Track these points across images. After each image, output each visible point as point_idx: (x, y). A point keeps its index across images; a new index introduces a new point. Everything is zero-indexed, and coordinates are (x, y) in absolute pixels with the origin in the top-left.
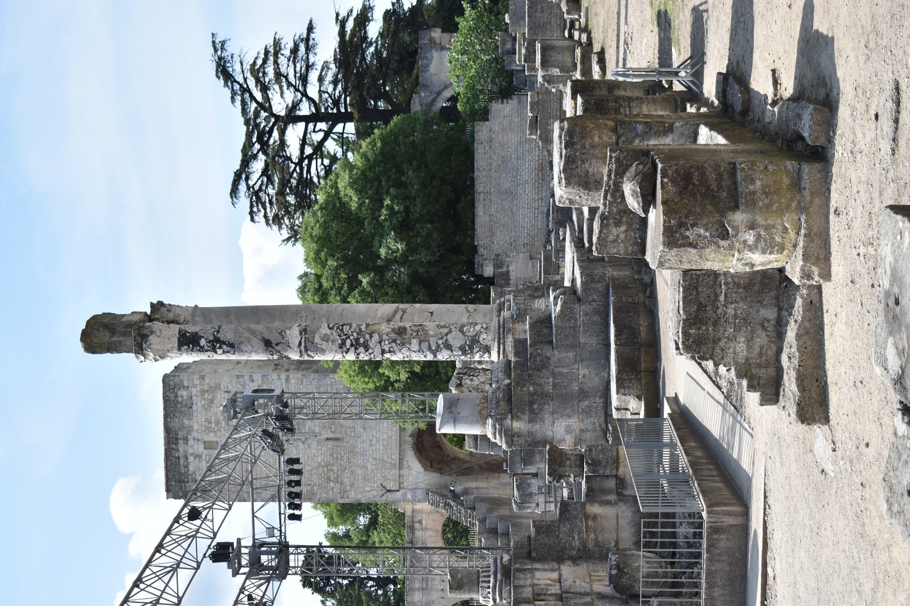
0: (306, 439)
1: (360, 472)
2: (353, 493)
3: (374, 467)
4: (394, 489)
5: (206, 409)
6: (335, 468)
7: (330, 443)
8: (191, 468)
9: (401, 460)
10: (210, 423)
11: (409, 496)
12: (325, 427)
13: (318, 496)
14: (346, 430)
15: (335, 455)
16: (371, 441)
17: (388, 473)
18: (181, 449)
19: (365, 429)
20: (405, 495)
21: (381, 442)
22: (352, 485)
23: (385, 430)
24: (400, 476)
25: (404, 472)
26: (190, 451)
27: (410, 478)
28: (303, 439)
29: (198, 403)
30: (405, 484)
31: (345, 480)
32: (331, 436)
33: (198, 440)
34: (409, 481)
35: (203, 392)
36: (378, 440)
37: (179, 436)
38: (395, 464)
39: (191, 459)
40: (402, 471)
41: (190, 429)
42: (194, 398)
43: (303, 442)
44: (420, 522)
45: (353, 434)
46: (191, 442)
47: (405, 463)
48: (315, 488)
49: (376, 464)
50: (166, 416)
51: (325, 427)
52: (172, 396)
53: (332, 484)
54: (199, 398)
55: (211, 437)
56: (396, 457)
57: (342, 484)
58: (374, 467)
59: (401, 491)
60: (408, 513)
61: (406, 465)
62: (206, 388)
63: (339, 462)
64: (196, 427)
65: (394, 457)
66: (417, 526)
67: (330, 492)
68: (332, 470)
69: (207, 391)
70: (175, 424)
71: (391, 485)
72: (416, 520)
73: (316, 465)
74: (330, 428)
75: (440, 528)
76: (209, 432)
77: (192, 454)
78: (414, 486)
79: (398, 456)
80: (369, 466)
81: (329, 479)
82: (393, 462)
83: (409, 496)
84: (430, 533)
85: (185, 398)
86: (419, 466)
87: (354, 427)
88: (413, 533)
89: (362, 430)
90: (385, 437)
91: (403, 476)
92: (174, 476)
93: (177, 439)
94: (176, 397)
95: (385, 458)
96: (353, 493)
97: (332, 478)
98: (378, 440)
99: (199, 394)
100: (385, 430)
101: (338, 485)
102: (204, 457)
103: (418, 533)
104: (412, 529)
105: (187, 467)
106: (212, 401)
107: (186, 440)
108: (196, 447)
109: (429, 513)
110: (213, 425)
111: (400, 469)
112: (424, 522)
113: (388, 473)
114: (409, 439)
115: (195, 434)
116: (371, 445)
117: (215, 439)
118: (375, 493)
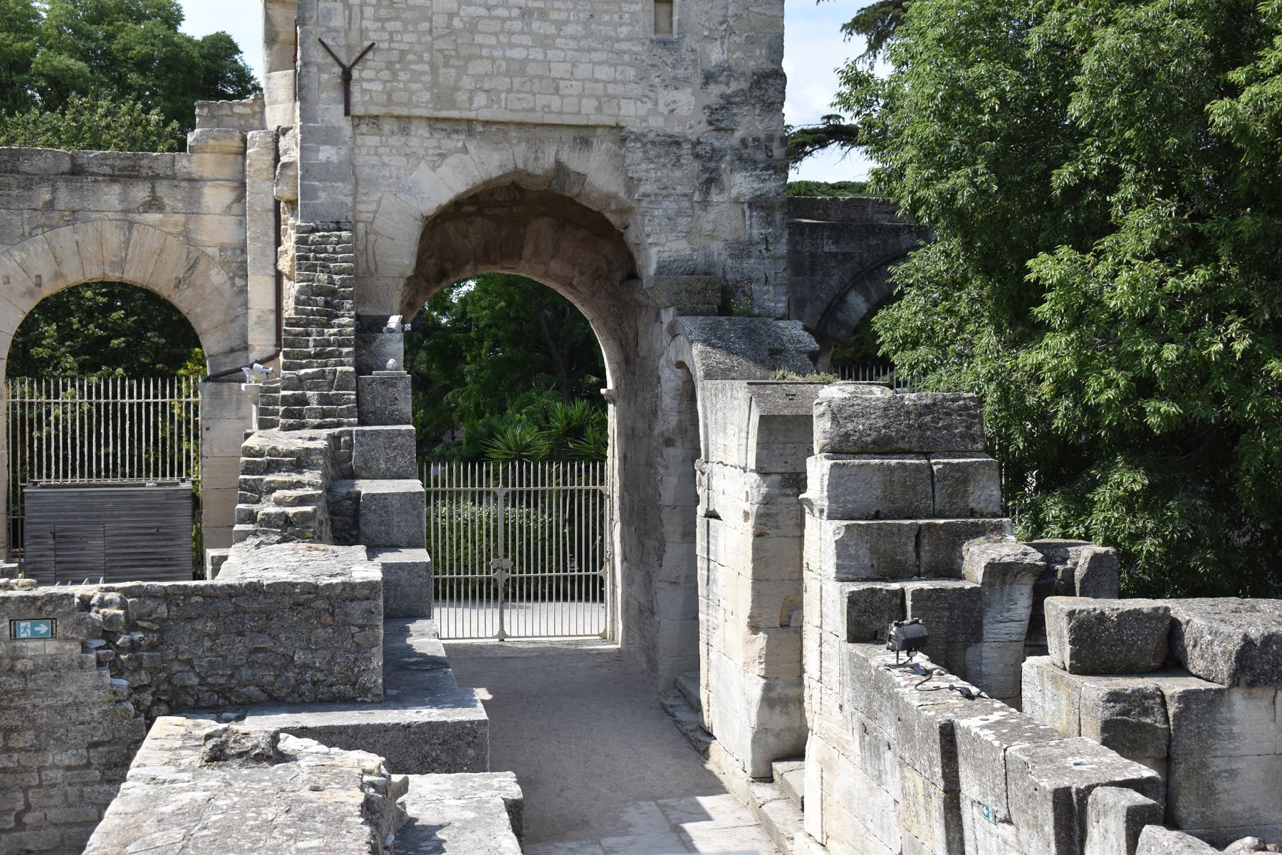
3: (439, 21)
4: (356, 97)
9: (468, 126)
11: (327, 153)
16: (543, 15)
17: (416, 76)
20: (330, 136)
21: (537, 54)
23: (583, 70)
24: (404, 121)
25: (420, 137)
27: (397, 161)
30: (373, 140)
36: (545, 42)
38: (453, 105)
40: (423, 131)
44: (154, 204)
47: (458, 141)
49: (451, 31)
56: (480, 108)
58: (439, 21)
59: (345, 124)
60: (184, 163)
61: (448, 144)
65: (481, 99)
66: (140, 193)
71: (370, 86)
72: (163, 189)
75: (133, 275)
78: (365, 172)
79: (485, 115)
82: (461, 97)
83: (327, 153)
84: (114, 238)
86: (444, 196)
88: (113, 178)
90: (559, 70)
91: (405, 131)
98: (545, 42)
100: (583, 70)
103: (111, 195)
104: (126, 176)
109: (187, 236)
111: (433, 122)
112: (153, 217)
113: (416, 76)
114: (547, 161)
118: (338, 21)
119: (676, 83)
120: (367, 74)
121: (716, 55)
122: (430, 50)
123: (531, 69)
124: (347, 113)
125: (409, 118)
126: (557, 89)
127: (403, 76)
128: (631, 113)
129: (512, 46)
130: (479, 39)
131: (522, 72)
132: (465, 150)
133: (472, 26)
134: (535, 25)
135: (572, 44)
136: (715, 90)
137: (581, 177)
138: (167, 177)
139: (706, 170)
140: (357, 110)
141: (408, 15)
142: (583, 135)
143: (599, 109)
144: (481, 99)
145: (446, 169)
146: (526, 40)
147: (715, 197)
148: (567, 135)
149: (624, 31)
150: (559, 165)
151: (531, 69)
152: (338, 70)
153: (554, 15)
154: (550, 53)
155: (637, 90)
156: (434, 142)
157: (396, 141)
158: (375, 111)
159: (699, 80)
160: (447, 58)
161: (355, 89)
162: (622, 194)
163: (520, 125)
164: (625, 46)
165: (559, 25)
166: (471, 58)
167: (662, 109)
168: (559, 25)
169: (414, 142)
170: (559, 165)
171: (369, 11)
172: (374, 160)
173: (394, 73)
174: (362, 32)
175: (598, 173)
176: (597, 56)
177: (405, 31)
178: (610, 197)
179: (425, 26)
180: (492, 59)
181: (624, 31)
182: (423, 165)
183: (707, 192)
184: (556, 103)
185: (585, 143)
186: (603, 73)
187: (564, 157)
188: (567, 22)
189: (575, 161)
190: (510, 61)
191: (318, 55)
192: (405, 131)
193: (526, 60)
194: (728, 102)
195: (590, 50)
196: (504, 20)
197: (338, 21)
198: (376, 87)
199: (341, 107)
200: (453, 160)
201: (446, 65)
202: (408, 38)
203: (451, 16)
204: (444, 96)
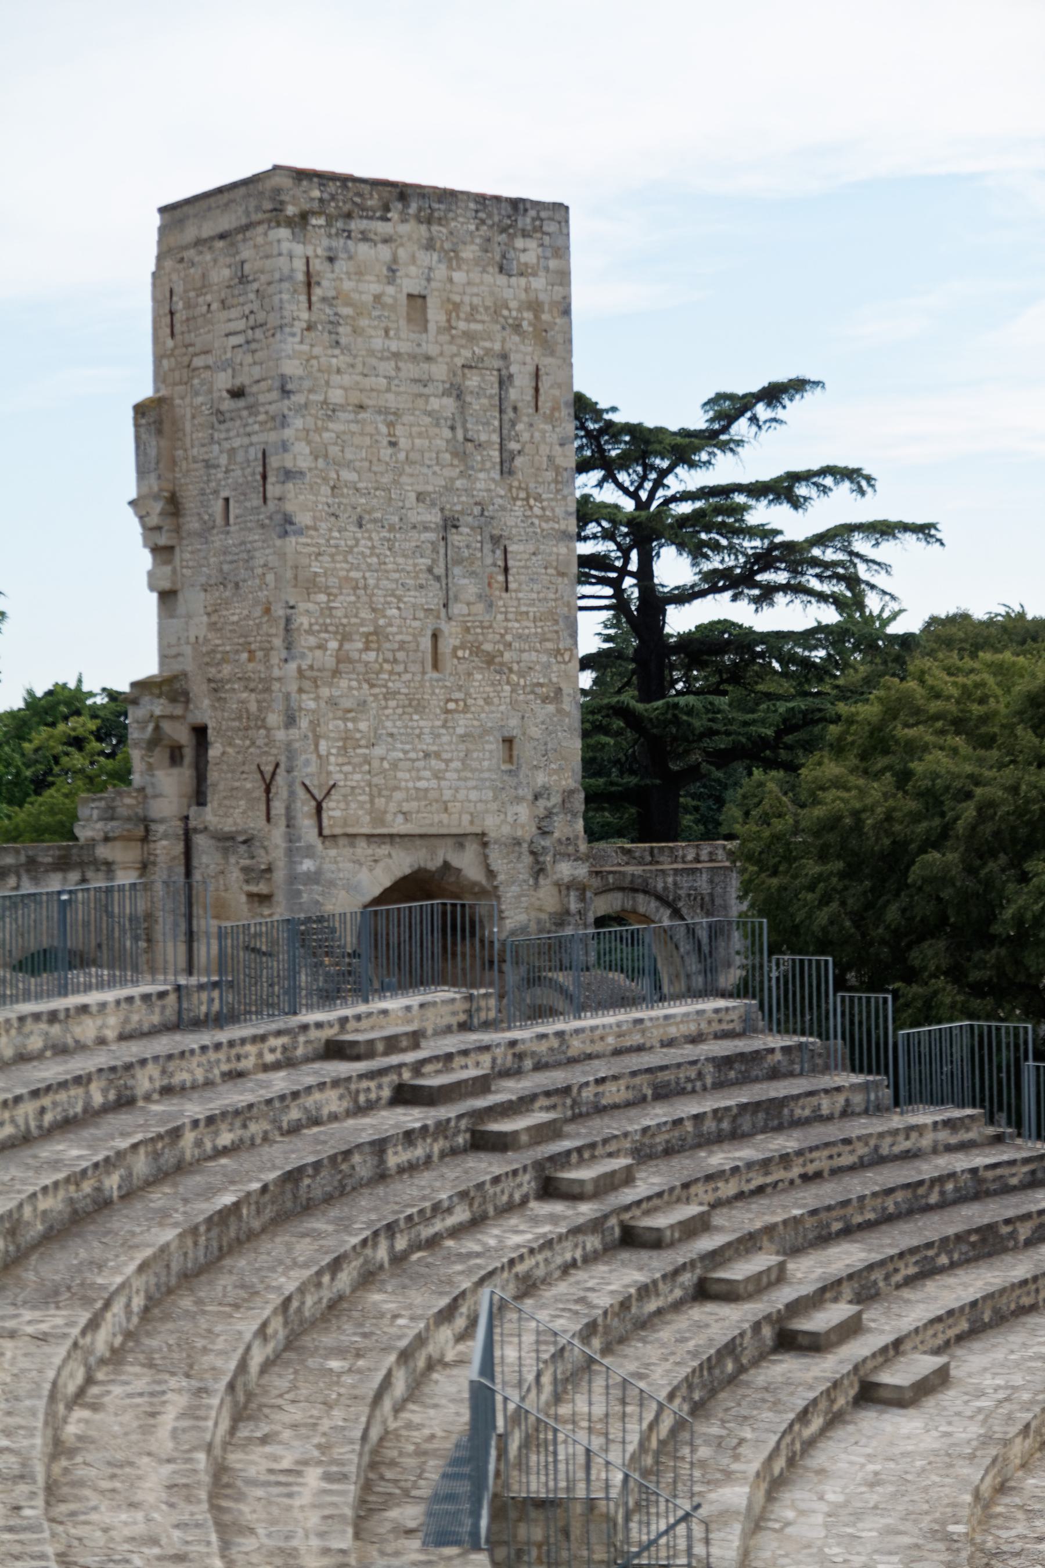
0: (438, 579)
1: (363, 726)
2: (312, 705)
3: (376, 763)
4: (325, 822)
5: (498, 309)
6: (371, 656)
7: (426, 643)
8: (363, 249)
10: (471, 318)
12: (467, 630)
13: (302, 606)
14: (460, 688)
15: (401, 655)
16: (437, 755)
17: (361, 805)
18: (404, 229)
19: (463, 738)
21: (434, 783)
22: (333, 702)
23: (461, 795)
26: (401, 252)
28: (436, 571)
29: (512, 290)
30: (333, 852)
31: (344, 683)
32: (447, 645)
33: (429, 280)
34: (337, 862)
35: (535, 306)
37: (435, 228)
38: (382, 822)
39: (384, 252)
40: (362, 843)
41: (452, 258)
42: (523, 281)
43: (430, 570)
45: (451, 706)
46: (426, 258)
47: (384, 850)
48: (322, 598)
50: (482, 200)
51: (467, 630)
52: (525, 222)
53: (333, 645)
54: (523, 296)
55: (435, 315)
56: (399, 826)
57: (336, 673)
62: (545, 317)
63: (386, 666)
64: (459, 277)
67: (312, 641)
68: (367, 649)
69: (537, 317)
70: (463, 223)
71: (333, 810)
73: (379, 600)
74: (463, 647)
76: (449, 314)
77: (395, 259)
80: (379, 751)
81: (345, 637)
82: (389, 817)
85: (524, 258)
87: (466, 709)
89: (460, 731)
90: (447, 794)
91: (353, 845)
92: (333, 197)
93: (429, 221)
94: (525, 234)
95: (398, 795)
96: (312, 705)
97: (347, 646)
98: (438, 776)
99: (532, 295)
101: (330, 662)
102: (390, 290)
105: (365, 238)
106: (517, 328)
107: (430, 245)
108: (413, 270)
110: (462, 325)
111: (369, 837)
114: (439, 862)
115: (441, 271)
116: (427, 755)
117: (432, 327)
119: (518, 800)
120: (332, 805)
121: (541, 779)
122: (370, 785)
123: (432, 795)
124: (320, 834)
125: (355, 836)
126: (446, 810)
127: (353, 805)
128: (491, 823)
129: (420, 779)
130: (400, 775)
131: (426, 798)
132: (390, 855)
133: (395, 765)
134: (433, 762)
135: (455, 776)
136: (542, 803)
137: (459, 870)
138: (90, 863)
139: (537, 862)
140: (326, 832)
141: (356, 760)
142: (459, 840)
143: (472, 823)
144: (400, 818)
145: (379, 870)
146: (427, 774)
147: (542, 881)
148: (450, 842)
149: (486, 763)
150: (446, 865)
151: (432, 795)
152: (313, 803)
153: (445, 756)
154: (443, 783)
155: (494, 806)
156: (370, 851)
157: (348, 851)
158: (338, 831)
159: (530, 797)
160: (380, 790)
161: (324, 815)
162: (484, 882)
163: (422, 836)
164: (486, 775)
165: (447, 762)
166: (396, 788)
167: (510, 819)
168: (447, 762)
169: (359, 851)
170: (446, 865)
171: (332, 759)
172: (333, 867)
173: (347, 803)
174: (329, 773)
175: (468, 864)
176: (471, 783)
177: (354, 772)
178: (475, 884)
179: (366, 767)
180: (407, 789)
181: (486, 763)
182: (365, 869)
183: (536, 879)
184: (444, 817)
185: (461, 846)
186: (474, 795)
187: (449, 859)
188: (451, 760)
189: (456, 861)
190: (417, 789)
191: (301, 793)
192: (353, 845)
193: (426, 790)
194: (549, 815)
195: (466, 779)
196: (413, 761)
197: (312, 769)
198: (337, 813)
199: (316, 831)
200: (381, 865)
201: (380, 795)
202: (358, 777)
203: (382, 759)
204: (379, 818)
